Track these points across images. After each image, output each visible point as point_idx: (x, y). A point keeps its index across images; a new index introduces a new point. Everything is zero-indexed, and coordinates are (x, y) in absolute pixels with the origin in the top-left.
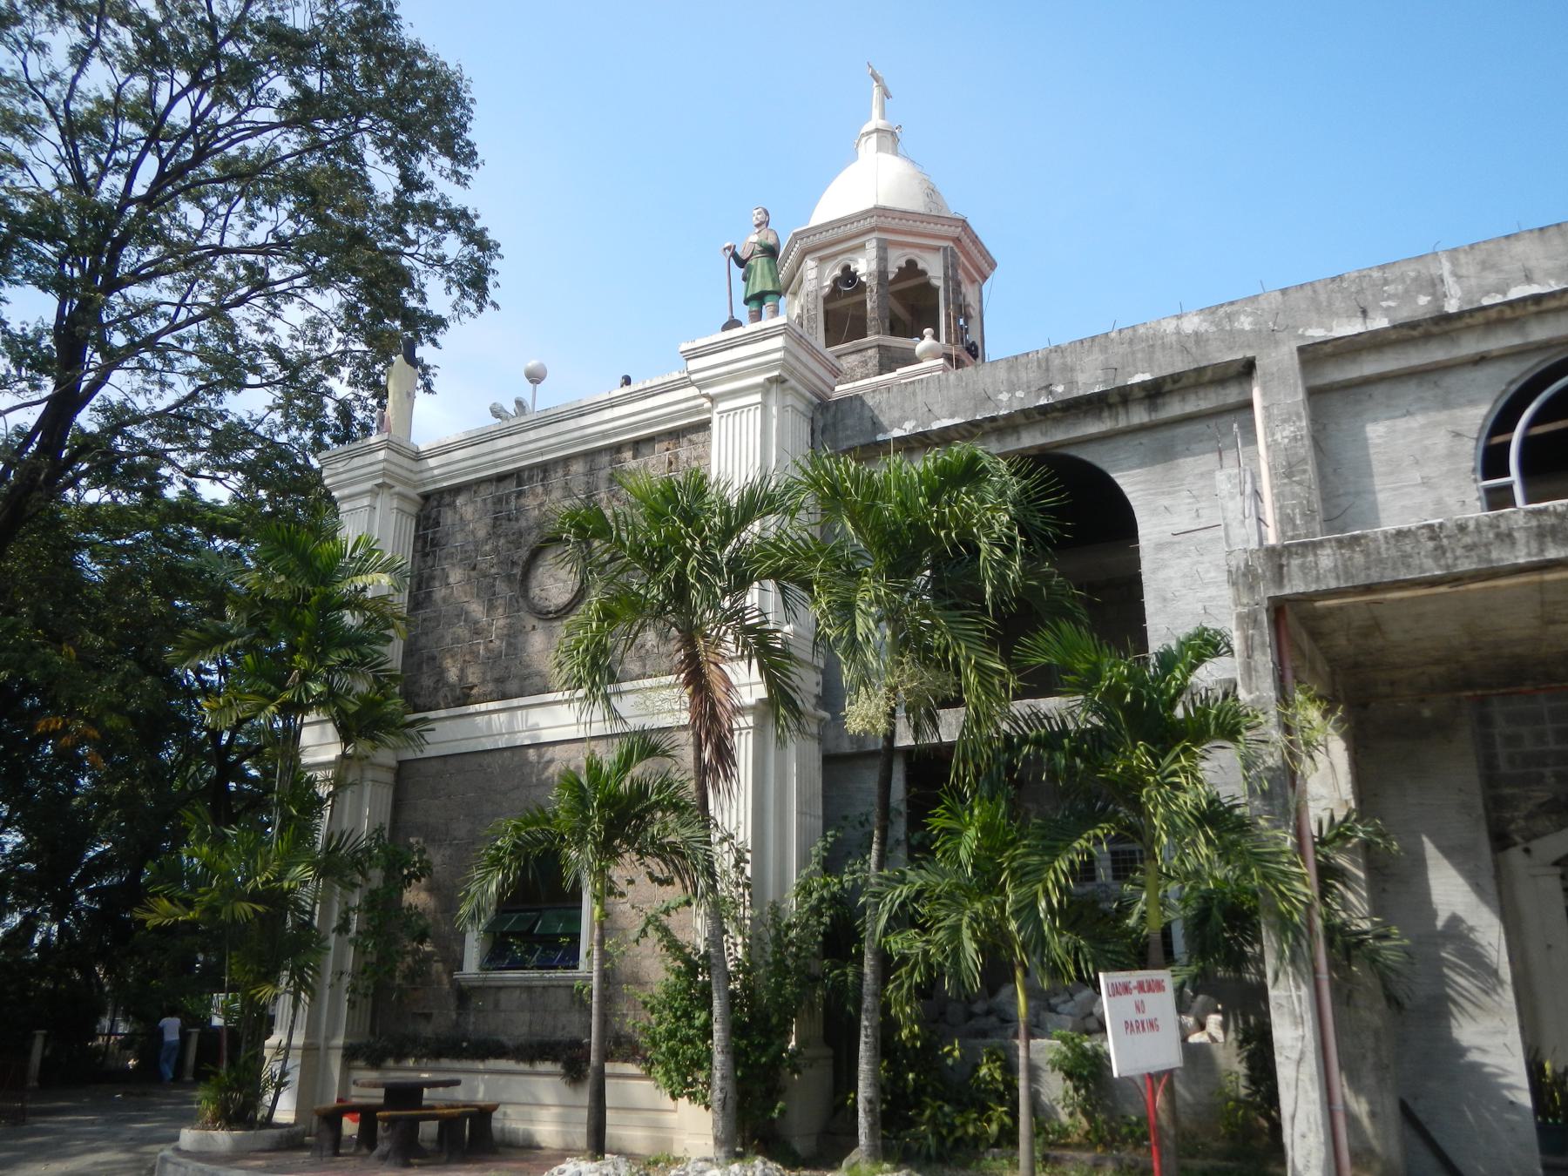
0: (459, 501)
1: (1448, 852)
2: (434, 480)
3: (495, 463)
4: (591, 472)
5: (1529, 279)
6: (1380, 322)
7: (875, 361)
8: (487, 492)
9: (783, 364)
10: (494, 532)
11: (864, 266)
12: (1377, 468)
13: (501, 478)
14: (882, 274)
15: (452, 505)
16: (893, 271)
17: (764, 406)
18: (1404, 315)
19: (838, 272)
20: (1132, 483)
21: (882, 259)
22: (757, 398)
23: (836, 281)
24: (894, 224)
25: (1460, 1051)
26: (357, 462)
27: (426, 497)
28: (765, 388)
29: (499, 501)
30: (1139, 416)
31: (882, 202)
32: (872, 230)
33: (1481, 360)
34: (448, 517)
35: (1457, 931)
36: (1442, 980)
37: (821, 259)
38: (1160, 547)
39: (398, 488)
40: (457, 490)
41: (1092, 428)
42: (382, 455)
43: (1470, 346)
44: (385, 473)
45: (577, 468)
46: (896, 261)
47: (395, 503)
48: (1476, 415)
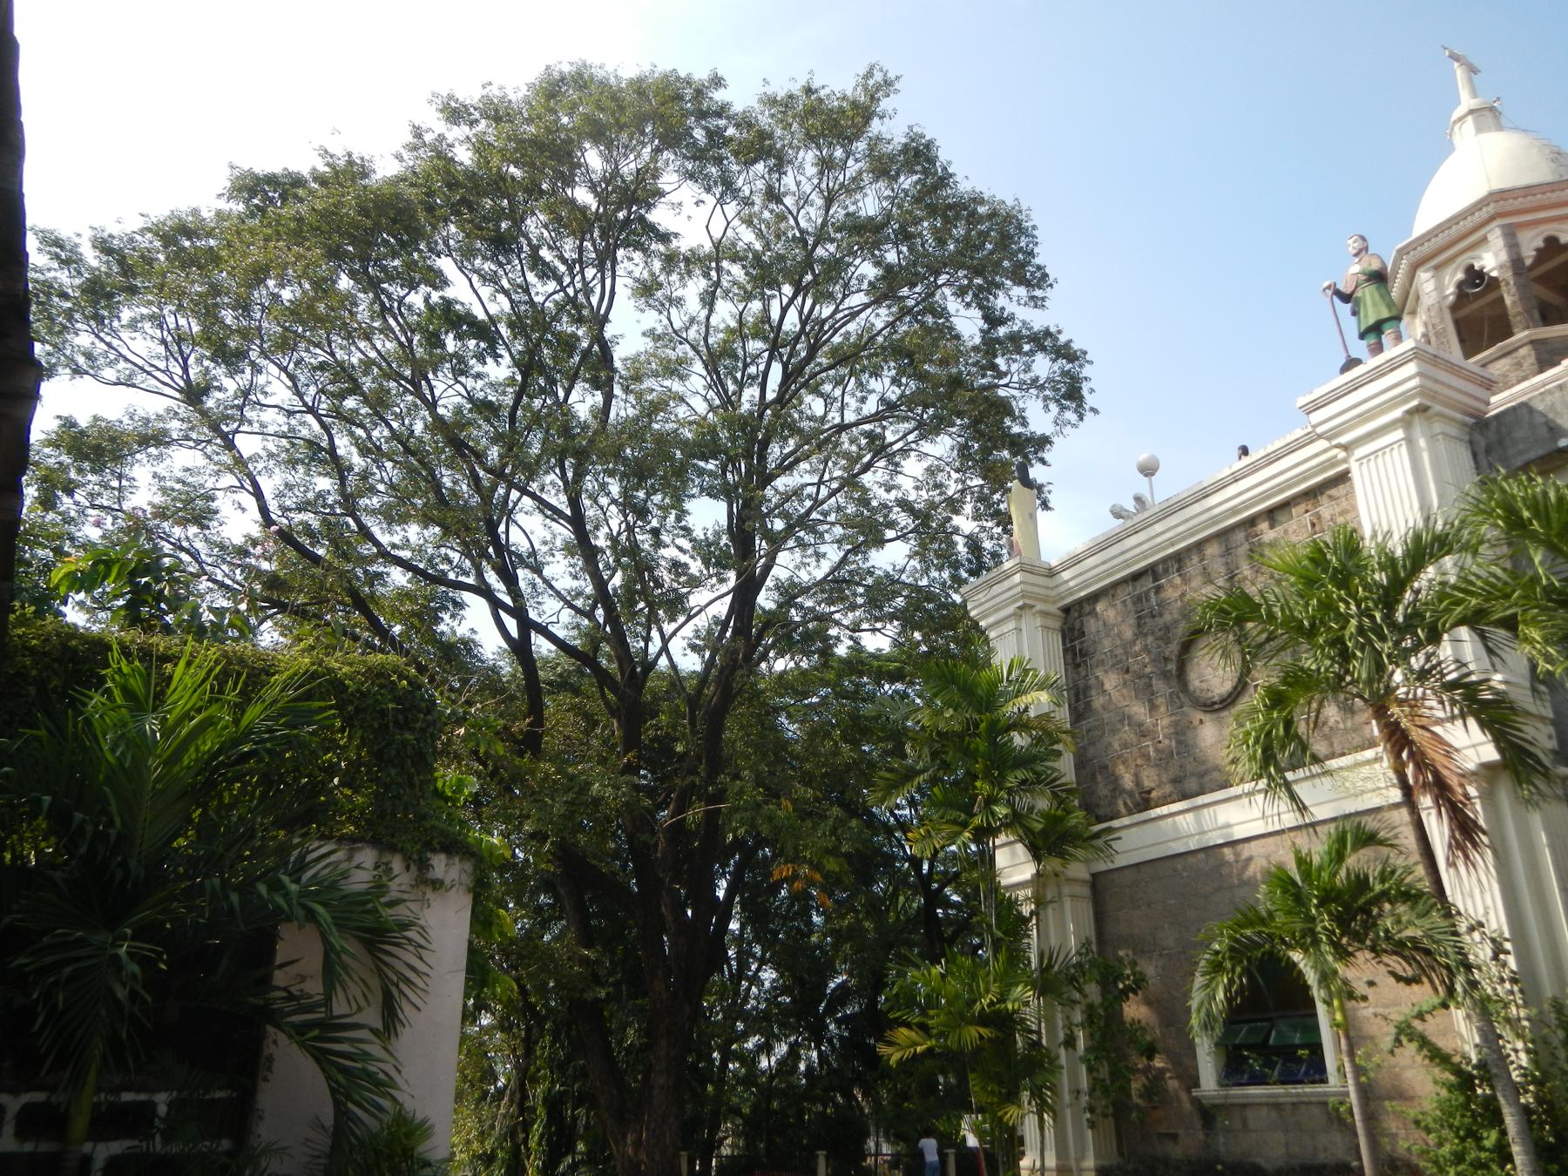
0: (1099, 607)
2: (1071, 592)
3: (1127, 564)
4: (1228, 551)
7: (1532, 359)
8: (1124, 594)
9: (1422, 391)
11: (1491, 260)
13: (1136, 577)
14: (1516, 263)
15: (1093, 613)
16: (1529, 255)
17: (1410, 441)
19: (1460, 276)
21: (1512, 245)
22: (1399, 434)
24: (1519, 203)
26: (997, 589)
27: (1066, 610)
28: (1406, 421)
29: (1138, 599)
31: (1497, 185)
32: (1492, 219)
34: (1092, 625)
37: (1437, 268)
39: (1039, 607)
40: (1094, 598)
42: (1017, 578)
44: (1024, 595)
45: (1213, 550)
46: (1531, 243)
47: (1039, 622)
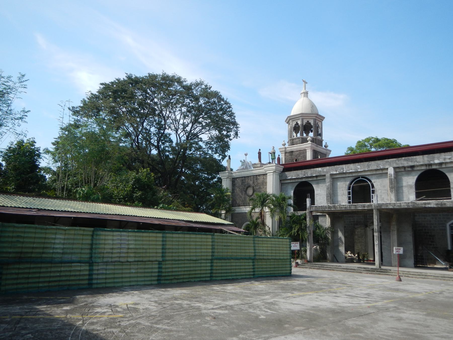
0: (237, 179)
1: (340, 230)
4: (254, 178)
5: (352, 170)
6: (338, 172)
8: (241, 179)
9: (275, 170)
10: (242, 185)
11: (299, 122)
12: (338, 188)
14: (302, 124)
16: (304, 124)
17: (273, 175)
18: (340, 172)
19: (295, 123)
20: (314, 186)
21: (302, 122)
23: (295, 124)
24: (305, 115)
25: (339, 250)
27: (233, 178)
28: (273, 172)
29: (242, 180)
30: (315, 179)
31: (301, 112)
32: (301, 117)
33: (349, 177)
34: (236, 181)
35: (340, 238)
36: (338, 243)
38: (317, 194)
40: (237, 178)
41: (310, 179)
43: (347, 175)
44: (228, 176)
45: (252, 177)
46: (305, 121)
48: (348, 183)
